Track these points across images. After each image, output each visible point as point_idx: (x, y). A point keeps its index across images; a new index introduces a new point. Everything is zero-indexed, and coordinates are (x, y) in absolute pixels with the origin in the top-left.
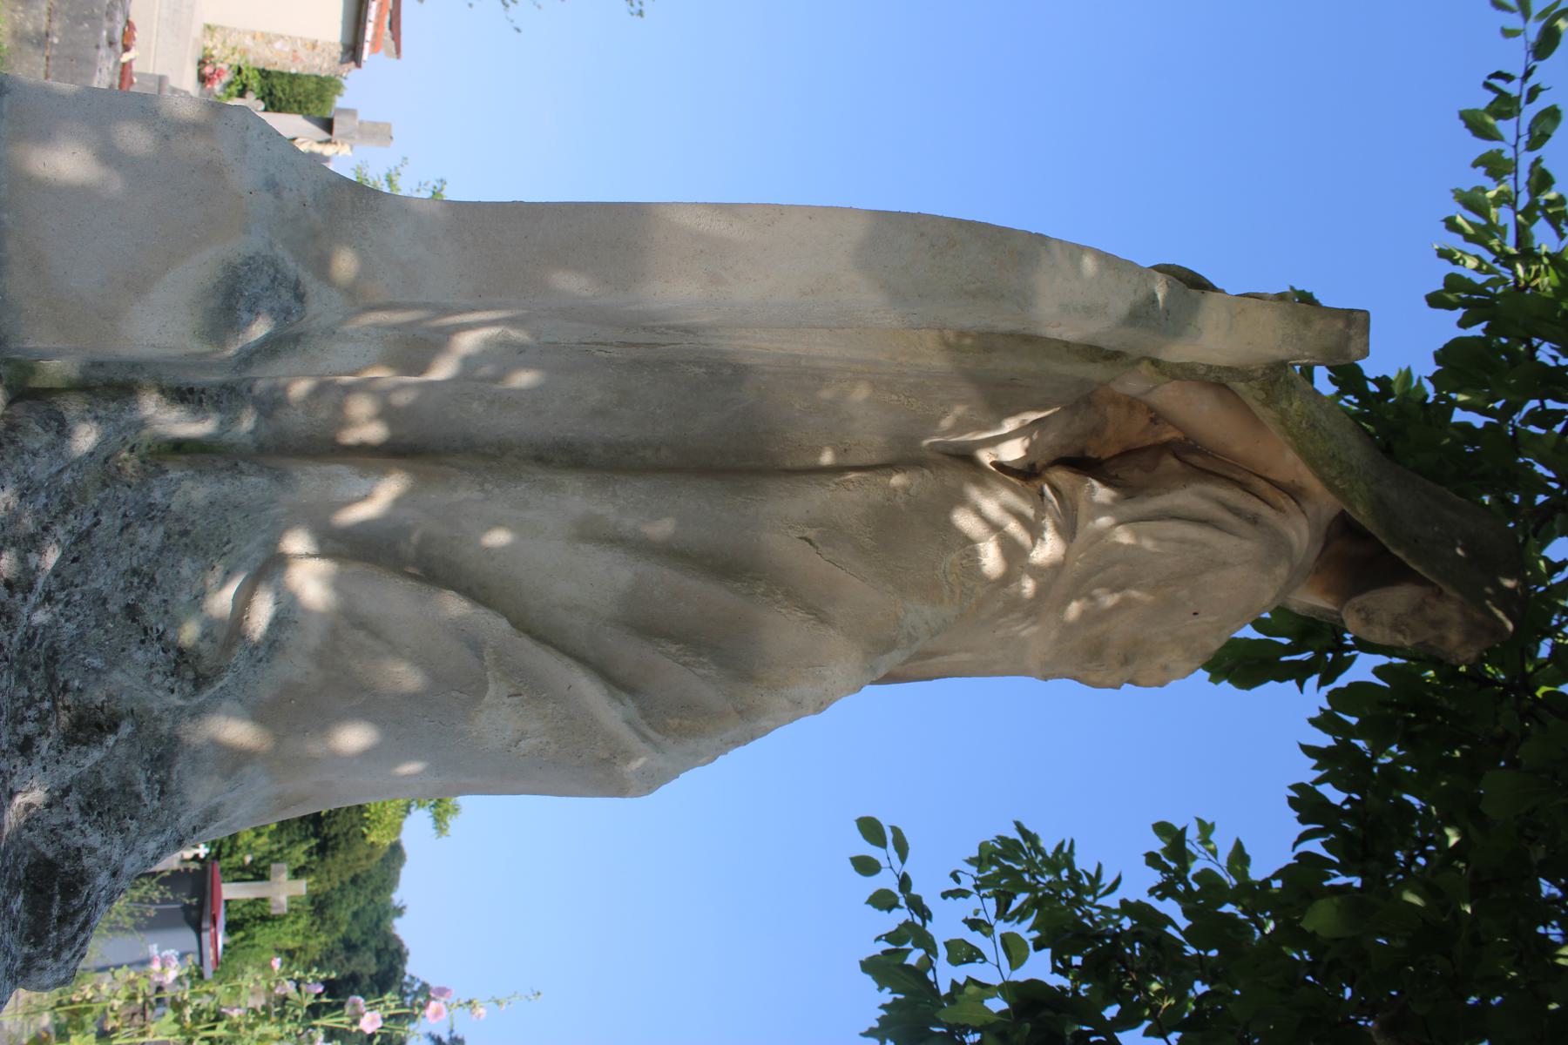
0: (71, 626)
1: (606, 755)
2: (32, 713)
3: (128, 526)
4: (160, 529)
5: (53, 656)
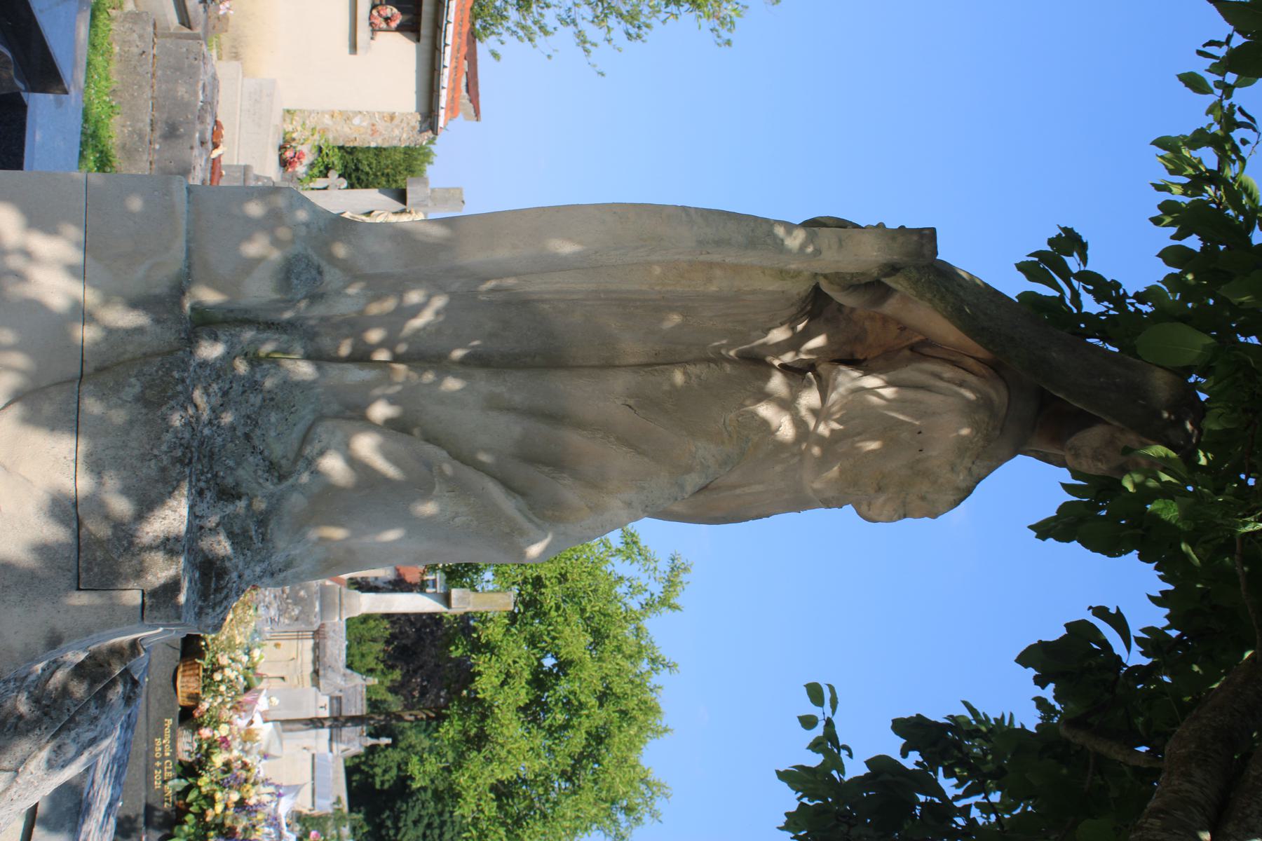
0: (220, 439)
1: (507, 530)
3: (244, 392)
4: (260, 396)
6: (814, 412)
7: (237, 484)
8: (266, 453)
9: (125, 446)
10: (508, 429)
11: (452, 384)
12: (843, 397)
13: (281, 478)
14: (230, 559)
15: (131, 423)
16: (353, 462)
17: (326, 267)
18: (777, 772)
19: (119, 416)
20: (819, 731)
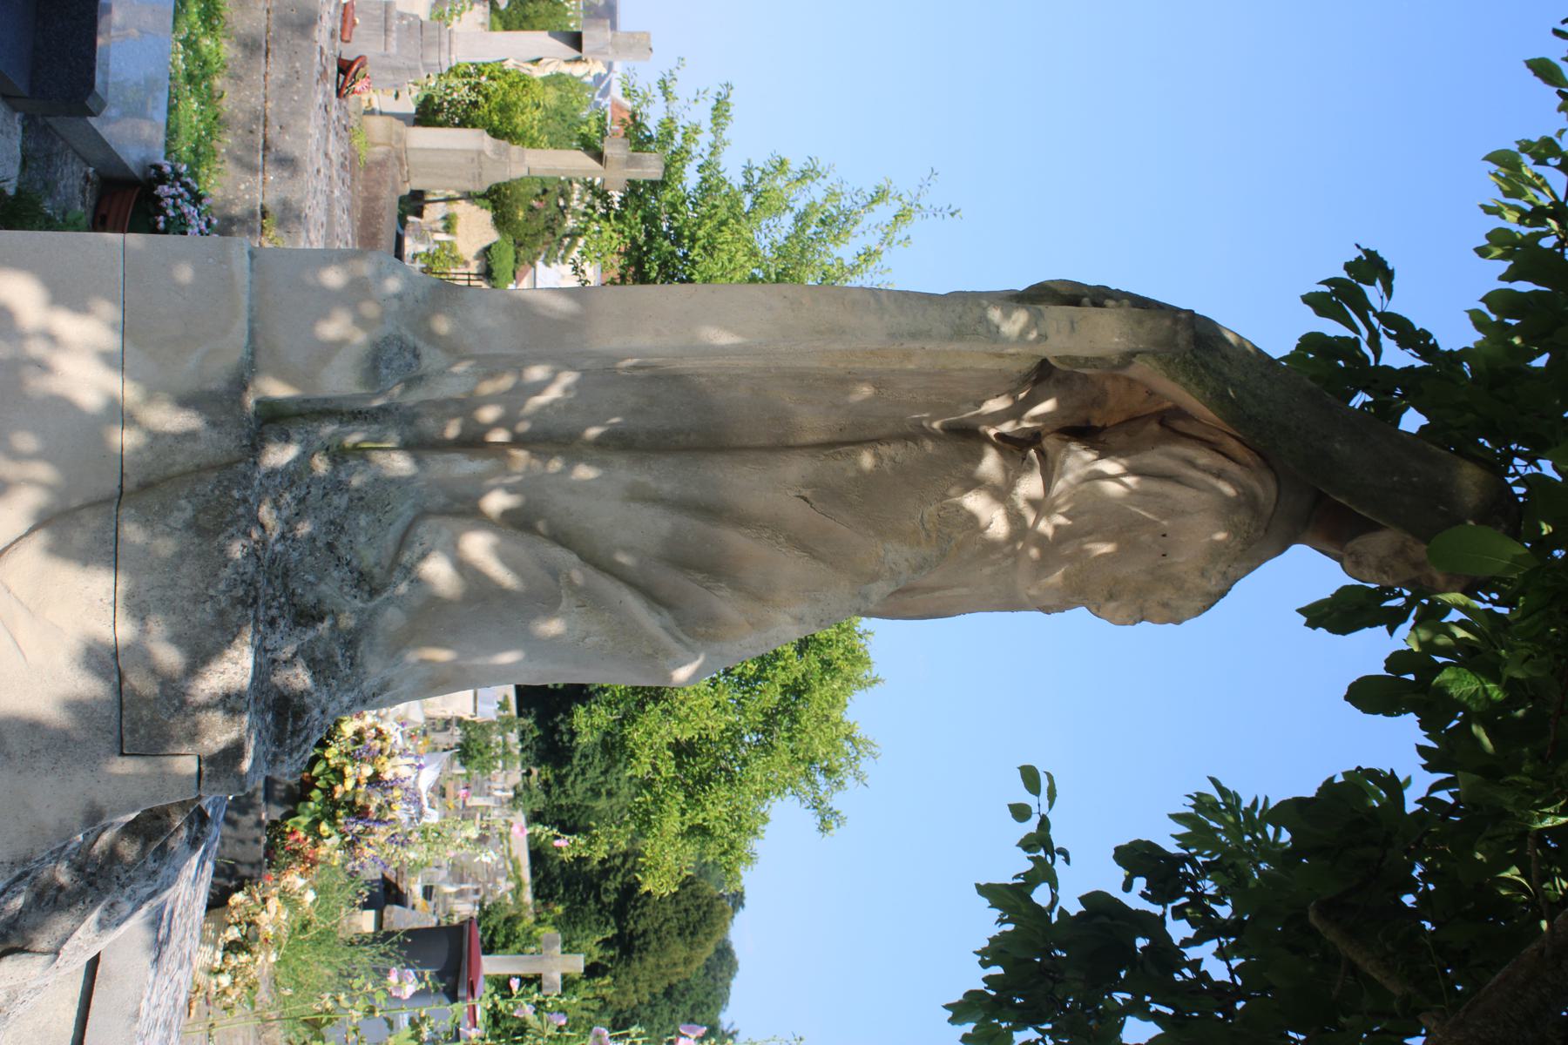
0: (296, 554)
2: (275, 604)
3: (325, 495)
4: (346, 497)
5: (286, 573)
6: (1034, 503)
7: (319, 601)
8: (355, 563)
9: (174, 585)
10: (656, 525)
11: (584, 472)
12: (1072, 486)
13: (373, 593)
14: (310, 694)
15: (181, 555)
16: (462, 566)
17: (422, 346)
18: (978, 886)
19: (166, 547)
20: (1031, 826)
